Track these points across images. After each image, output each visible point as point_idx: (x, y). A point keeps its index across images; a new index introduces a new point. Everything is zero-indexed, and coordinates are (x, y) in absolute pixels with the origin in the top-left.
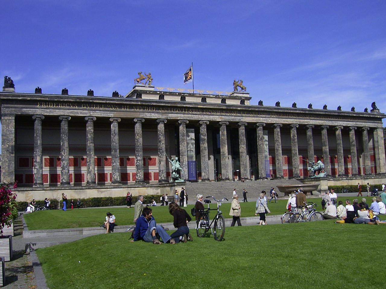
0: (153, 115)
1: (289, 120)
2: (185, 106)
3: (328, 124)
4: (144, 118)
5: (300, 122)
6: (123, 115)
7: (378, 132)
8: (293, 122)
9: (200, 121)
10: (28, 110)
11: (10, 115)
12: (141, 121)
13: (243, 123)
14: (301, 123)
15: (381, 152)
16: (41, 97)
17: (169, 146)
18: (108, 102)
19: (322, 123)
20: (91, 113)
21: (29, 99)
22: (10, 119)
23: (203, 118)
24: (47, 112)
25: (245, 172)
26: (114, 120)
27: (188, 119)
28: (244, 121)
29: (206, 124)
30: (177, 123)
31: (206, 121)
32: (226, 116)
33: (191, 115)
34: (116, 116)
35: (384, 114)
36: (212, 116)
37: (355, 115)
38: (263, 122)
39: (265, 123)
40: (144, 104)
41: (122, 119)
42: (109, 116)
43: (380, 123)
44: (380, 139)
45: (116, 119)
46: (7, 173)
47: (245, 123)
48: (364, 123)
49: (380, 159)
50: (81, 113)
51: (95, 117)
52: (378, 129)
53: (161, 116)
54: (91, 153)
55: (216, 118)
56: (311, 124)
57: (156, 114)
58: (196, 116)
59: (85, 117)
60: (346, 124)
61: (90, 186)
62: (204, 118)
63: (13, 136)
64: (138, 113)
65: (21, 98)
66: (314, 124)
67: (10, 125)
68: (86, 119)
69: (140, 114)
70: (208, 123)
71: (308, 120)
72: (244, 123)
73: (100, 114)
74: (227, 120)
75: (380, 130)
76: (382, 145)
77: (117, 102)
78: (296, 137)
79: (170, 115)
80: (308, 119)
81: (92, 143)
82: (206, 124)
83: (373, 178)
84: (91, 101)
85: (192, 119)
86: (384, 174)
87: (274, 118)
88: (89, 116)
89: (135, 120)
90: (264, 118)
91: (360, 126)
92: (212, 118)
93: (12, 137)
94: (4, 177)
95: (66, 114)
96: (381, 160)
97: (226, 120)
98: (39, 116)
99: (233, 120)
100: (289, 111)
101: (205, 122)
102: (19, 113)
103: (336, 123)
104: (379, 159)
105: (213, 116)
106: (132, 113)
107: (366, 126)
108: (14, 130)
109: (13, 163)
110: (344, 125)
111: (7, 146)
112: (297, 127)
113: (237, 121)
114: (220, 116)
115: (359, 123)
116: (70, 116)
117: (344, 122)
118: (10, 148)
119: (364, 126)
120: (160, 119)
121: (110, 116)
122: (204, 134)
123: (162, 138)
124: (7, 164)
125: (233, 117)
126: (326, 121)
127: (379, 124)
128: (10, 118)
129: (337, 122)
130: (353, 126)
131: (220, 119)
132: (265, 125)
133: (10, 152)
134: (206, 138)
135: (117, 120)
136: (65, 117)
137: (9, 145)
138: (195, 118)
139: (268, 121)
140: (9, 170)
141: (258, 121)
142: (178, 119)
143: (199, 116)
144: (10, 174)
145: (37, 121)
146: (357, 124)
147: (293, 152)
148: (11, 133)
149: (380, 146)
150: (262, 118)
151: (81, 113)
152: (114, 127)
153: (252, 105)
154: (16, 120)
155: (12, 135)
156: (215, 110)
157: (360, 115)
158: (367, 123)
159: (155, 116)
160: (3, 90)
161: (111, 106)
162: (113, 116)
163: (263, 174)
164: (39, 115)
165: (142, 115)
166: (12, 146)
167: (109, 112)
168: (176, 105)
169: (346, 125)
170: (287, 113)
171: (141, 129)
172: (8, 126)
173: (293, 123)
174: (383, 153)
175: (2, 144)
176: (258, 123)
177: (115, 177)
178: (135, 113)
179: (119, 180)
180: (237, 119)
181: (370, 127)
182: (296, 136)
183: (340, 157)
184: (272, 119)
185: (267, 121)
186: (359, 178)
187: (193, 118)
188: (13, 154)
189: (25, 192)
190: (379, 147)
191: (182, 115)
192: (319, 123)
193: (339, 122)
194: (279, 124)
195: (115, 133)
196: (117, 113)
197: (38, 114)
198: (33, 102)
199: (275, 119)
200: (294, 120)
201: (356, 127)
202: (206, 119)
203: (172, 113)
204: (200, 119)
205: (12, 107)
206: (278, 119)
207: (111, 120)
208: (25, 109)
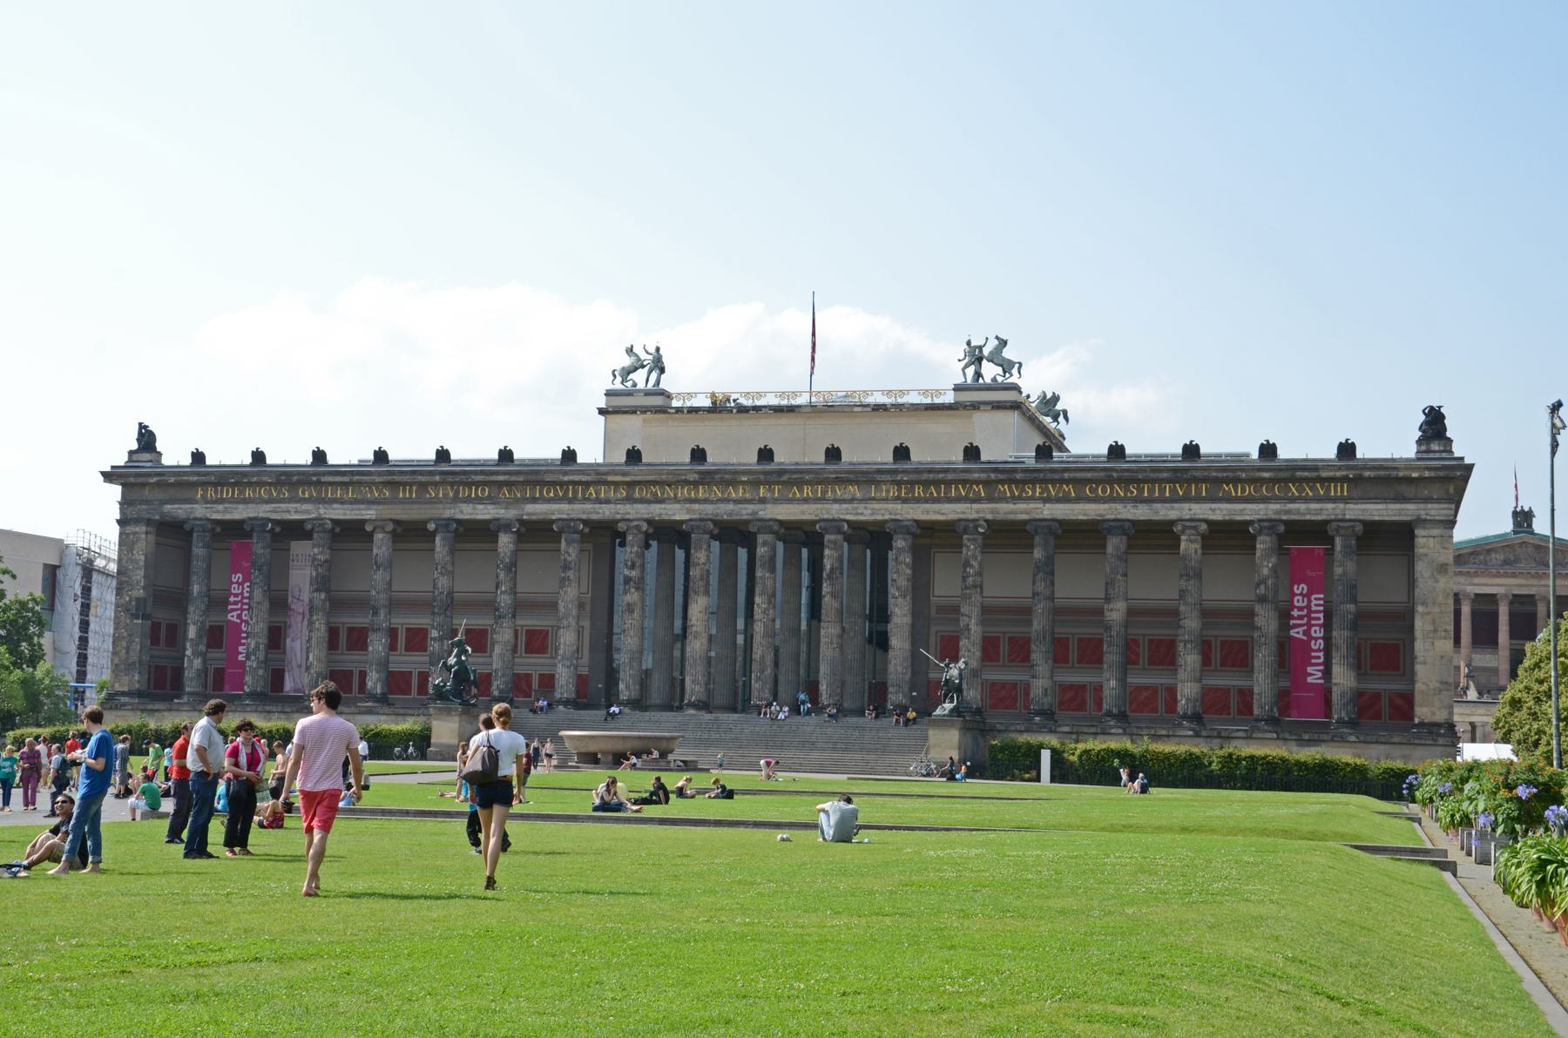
0: (484, 512)
1: (946, 507)
2: (566, 478)
3: (1130, 517)
4: (459, 522)
5: (998, 513)
6: (399, 512)
7: (1419, 541)
8: (964, 513)
9: (619, 521)
10: (178, 510)
11: (137, 521)
12: (447, 526)
14: (1000, 517)
15: (1431, 628)
16: (198, 474)
17: (589, 595)
18: (356, 478)
19: (1102, 512)
20: (322, 511)
21: (172, 480)
22: (135, 533)
23: (629, 513)
24: (218, 512)
25: (757, 685)
26: (374, 528)
27: (584, 517)
28: (768, 517)
29: (640, 532)
30: (587, 530)
31: (638, 520)
32: (706, 501)
33: (591, 506)
34: (384, 516)
35: (1462, 459)
36: (658, 506)
37: (1266, 475)
38: (842, 517)
39: (848, 522)
40: (450, 479)
41: (396, 522)
42: (364, 517)
43: (1439, 501)
44: (1426, 574)
45: (380, 523)
46: (122, 667)
47: (771, 523)
48: (1330, 506)
49: (1420, 659)
51: (333, 521)
52: (1425, 528)
53: (503, 511)
54: (315, 617)
55: (670, 513)
56: (1049, 517)
57: (489, 507)
58: (608, 506)
59: (303, 521)
60: (1225, 512)
62: (633, 512)
64: (441, 506)
65: (154, 480)
66: (1060, 517)
67: (136, 546)
68: (309, 527)
69: (444, 509)
71: (1032, 506)
72: (771, 523)
73: (341, 512)
74: (711, 517)
75: (1436, 532)
76: (1440, 599)
77: (378, 479)
78: (971, 566)
80: (1032, 499)
81: (317, 590)
82: (640, 532)
83: (1353, 738)
84: (314, 479)
85: (594, 517)
86: (1435, 729)
87: (886, 500)
88: (315, 519)
89: (431, 527)
90: (845, 506)
91: (1308, 517)
92: (658, 511)
93: (138, 577)
94: (117, 675)
95: (262, 515)
96: (1425, 663)
97: (706, 517)
98: (200, 523)
99: (730, 514)
100: (941, 476)
101: (635, 523)
102: (157, 517)
103: (1173, 509)
104: (1413, 658)
105: (663, 506)
106: (423, 506)
107: (1348, 517)
108: (143, 558)
110: (1212, 517)
111: (127, 599)
112: (981, 530)
113: (745, 517)
114: (687, 505)
115: (1303, 506)
116: (276, 522)
117: (1214, 506)
118: (134, 603)
119: (1333, 517)
120: (498, 520)
121: (367, 517)
122: (629, 563)
124: (124, 644)
125: (731, 507)
126: (1119, 506)
127: (1430, 506)
128: (137, 529)
129: (1176, 505)
130: (1265, 517)
131: (687, 513)
133: (132, 614)
135: (383, 528)
136: (260, 523)
137: (131, 597)
138: (604, 513)
139: (862, 514)
140: (127, 659)
141: (821, 517)
142: (554, 517)
143: (619, 506)
145: (195, 535)
146: (1288, 512)
147: (963, 621)
148: (136, 566)
149: (1424, 604)
150: (836, 506)
151: (296, 512)
152: (381, 545)
153: (797, 464)
155: (139, 572)
156: (669, 486)
157: (1299, 474)
158: (1351, 506)
159: (485, 511)
160: (126, 459)
161: (370, 488)
162: (374, 517)
163: (824, 697)
164: (201, 519)
165: (448, 513)
166: (138, 599)
167: (363, 506)
168: (540, 478)
169: (1227, 518)
170: (937, 483)
172: (131, 550)
173: (962, 516)
174: (1443, 634)
175: (117, 595)
176: (823, 524)
177: (369, 684)
178: (430, 506)
179: (379, 691)
180: (744, 512)
181: (1365, 523)
183: (1182, 645)
184: (876, 506)
185: (858, 514)
186: (1269, 735)
187: (598, 513)
188: (138, 618)
189: (156, 714)
190: (1420, 609)
191: (565, 507)
192: (1085, 514)
193: (1186, 506)
194: (905, 523)
195: (376, 562)
196: (386, 507)
197: (198, 516)
199: (891, 506)
200: (969, 505)
201: (1286, 523)
202: (639, 516)
203: (534, 500)
204: (619, 517)
205: (142, 502)
206: (899, 506)
207: (369, 528)
208: (169, 506)
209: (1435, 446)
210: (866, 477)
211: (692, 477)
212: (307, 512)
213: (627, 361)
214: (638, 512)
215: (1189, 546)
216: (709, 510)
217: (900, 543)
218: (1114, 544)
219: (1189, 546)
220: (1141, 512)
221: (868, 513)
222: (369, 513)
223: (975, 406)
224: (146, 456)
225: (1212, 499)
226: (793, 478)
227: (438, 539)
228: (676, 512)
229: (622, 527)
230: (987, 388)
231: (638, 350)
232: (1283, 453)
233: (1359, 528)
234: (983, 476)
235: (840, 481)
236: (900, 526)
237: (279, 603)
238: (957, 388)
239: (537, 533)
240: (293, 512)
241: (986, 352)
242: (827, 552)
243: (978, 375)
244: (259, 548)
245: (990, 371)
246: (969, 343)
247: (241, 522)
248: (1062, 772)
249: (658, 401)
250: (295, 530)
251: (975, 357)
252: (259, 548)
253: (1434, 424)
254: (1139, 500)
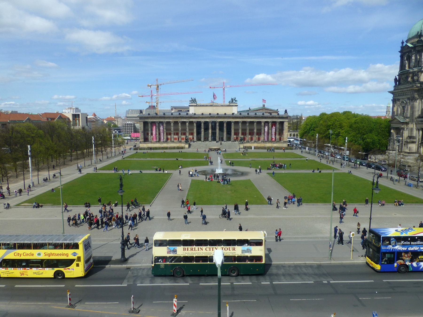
0: (185, 120)
11: (142, 122)
13: (218, 122)
16: (149, 116)
50: (162, 120)
61: (164, 142)
63: (142, 128)
68: (163, 122)
70: (204, 122)
79: (190, 120)
89: (179, 122)
109: (143, 135)
116: (159, 122)
123: (187, 127)
125: (214, 120)
128: (142, 123)
132: (227, 122)
134: (203, 127)
144: (142, 139)
146: (273, 120)
151: (162, 120)
152: (172, 124)
154: (143, 123)
171: (180, 125)
182: (241, 126)
198: (147, 118)
207: (171, 122)
209: (286, 114)
211: (210, 117)
212: (163, 120)
213: (191, 99)
214: (203, 120)
215: (263, 124)
217: (233, 124)
218: (255, 124)
219: (263, 124)
221: (229, 120)
222: (171, 120)
223: (233, 106)
224: (142, 114)
227: (179, 123)
228: (207, 120)
229: (201, 122)
231: (192, 98)
233: (279, 122)
234: (242, 117)
236: (233, 122)
237: (159, 130)
239: (191, 123)
240: (161, 120)
241: (234, 99)
242: (224, 125)
243: (233, 101)
244: (157, 124)
246: (232, 98)
247: (155, 122)
249: (196, 104)
250: (162, 123)
252: (157, 124)
253: (286, 111)
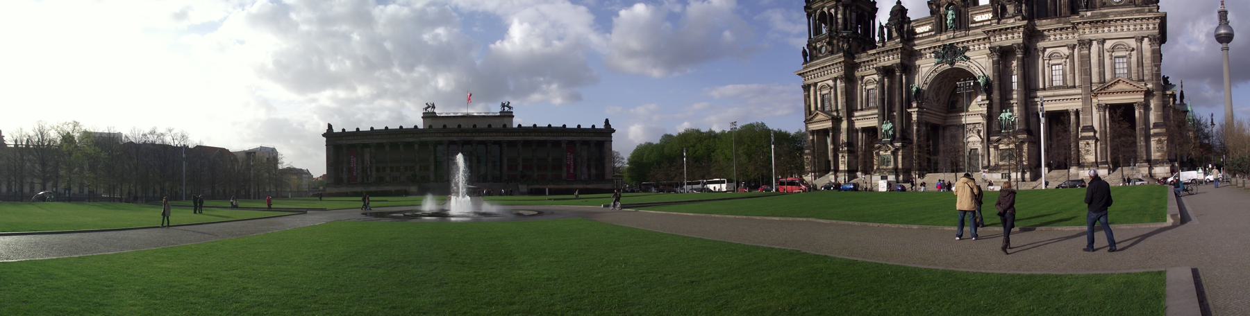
210: (497, 131)
215: (564, 145)
216: (462, 138)
220: (555, 139)
223: (504, 116)
225: (568, 136)
226: (481, 131)
230: (506, 112)
232: (582, 127)
235: (492, 132)
238: (500, 112)
243: (504, 109)
245: (506, 109)
248: (550, 193)
251: (503, 105)
253: (607, 121)
254: (554, 136)
